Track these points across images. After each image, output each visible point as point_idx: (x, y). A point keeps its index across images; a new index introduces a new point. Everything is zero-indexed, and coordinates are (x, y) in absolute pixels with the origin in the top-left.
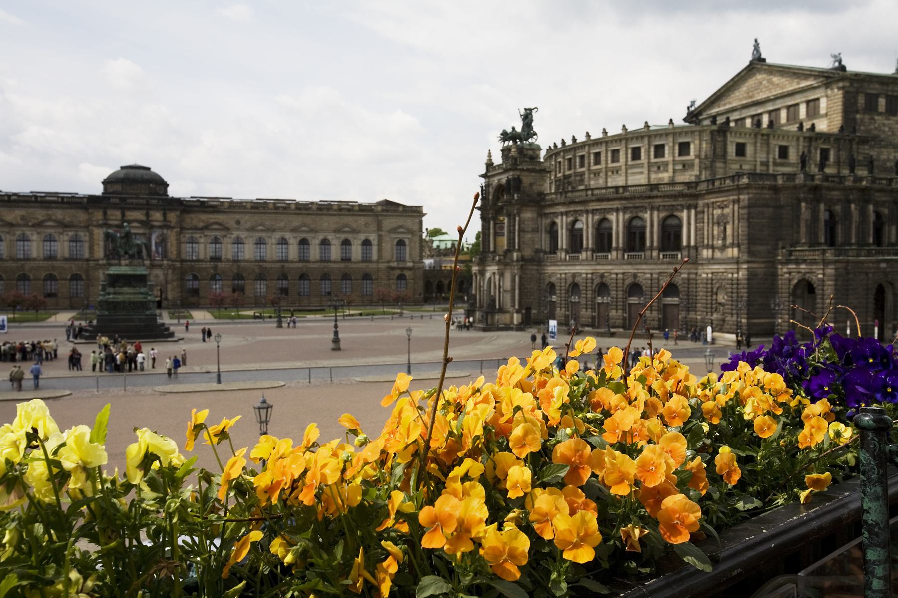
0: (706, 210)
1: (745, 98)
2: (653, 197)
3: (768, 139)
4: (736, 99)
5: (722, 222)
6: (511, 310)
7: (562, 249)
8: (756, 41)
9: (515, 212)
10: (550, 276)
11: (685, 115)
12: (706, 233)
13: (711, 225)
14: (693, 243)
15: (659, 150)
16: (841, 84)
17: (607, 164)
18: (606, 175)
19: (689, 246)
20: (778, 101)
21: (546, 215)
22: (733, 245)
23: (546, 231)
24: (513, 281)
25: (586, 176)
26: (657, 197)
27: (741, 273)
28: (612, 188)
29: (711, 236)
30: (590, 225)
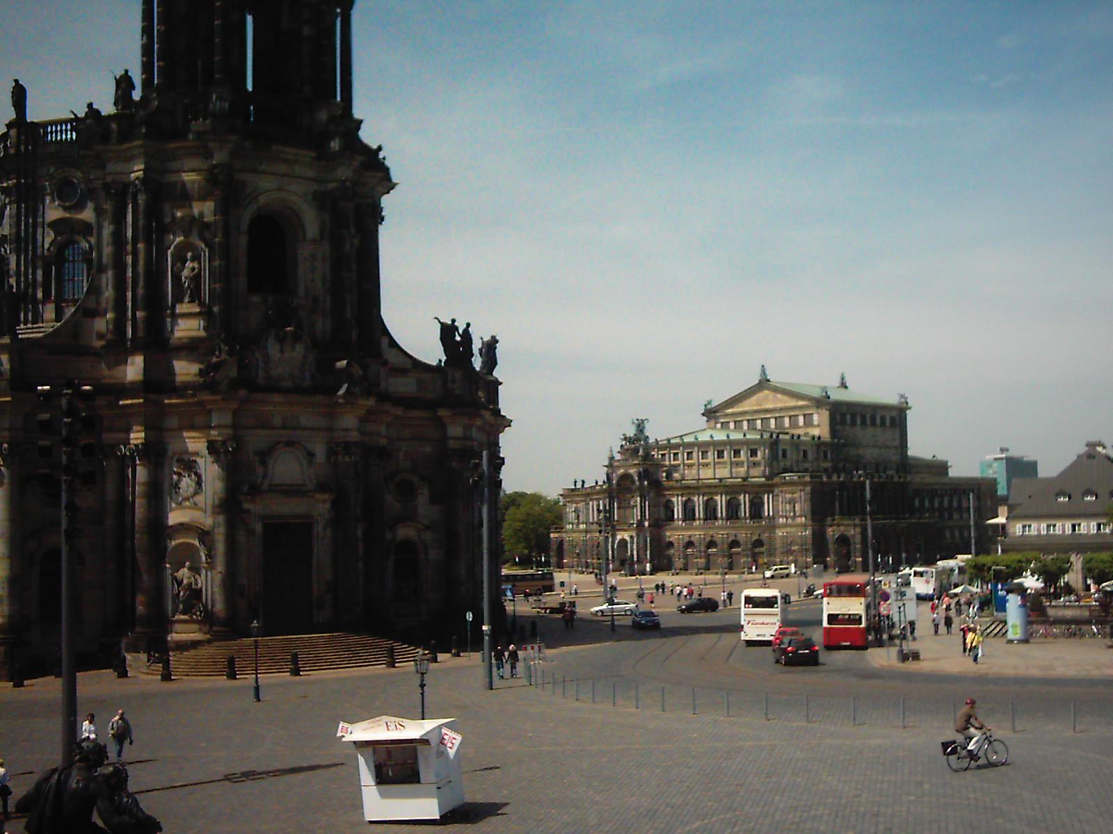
1: (755, 405)
4: (748, 405)
5: (792, 502)
8: (763, 366)
9: (646, 493)
10: (669, 537)
12: (780, 508)
13: (784, 504)
14: (771, 514)
15: (737, 453)
22: (801, 516)
25: (682, 466)
27: (807, 532)
28: (718, 479)
29: (784, 511)
30: (701, 503)
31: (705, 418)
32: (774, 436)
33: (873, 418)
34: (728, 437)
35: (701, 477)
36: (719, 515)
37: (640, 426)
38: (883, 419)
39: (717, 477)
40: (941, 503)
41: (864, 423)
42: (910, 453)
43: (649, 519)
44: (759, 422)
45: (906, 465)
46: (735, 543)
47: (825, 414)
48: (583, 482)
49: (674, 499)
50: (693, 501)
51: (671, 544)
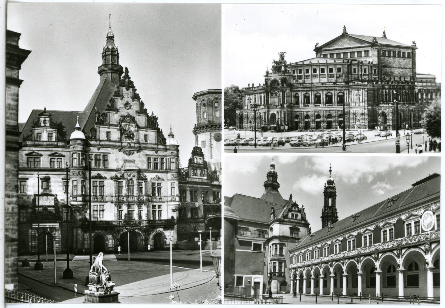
0: (352, 91)
2: (335, 86)
3: (361, 67)
6: (284, 124)
7: (301, 103)
8: (344, 26)
11: (314, 49)
13: (354, 96)
14: (348, 101)
16: (376, 47)
17: (312, 73)
18: (312, 77)
19: (347, 102)
20: (354, 49)
21: (294, 91)
23: (293, 97)
24: (285, 114)
25: (303, 76)
26: (337, 86)
31: (315, 52)
32: (350, 62)
33: (399, 53)
34: (327, 62)
35: (313, 82)
36: (322, 101)
37: (282, 56)
38: (404, 53)
39: (322, 81)
40: (431, 96)
41: (394, 56)
42: (417, 71)
43: (286, 103)
44: (342, 55)
45: (414, 78)
46: (330, 116)
47: (376, 52)
48: (253, 84)
49: (300, 93)
50: (309, 94)
51: (297, 117)
